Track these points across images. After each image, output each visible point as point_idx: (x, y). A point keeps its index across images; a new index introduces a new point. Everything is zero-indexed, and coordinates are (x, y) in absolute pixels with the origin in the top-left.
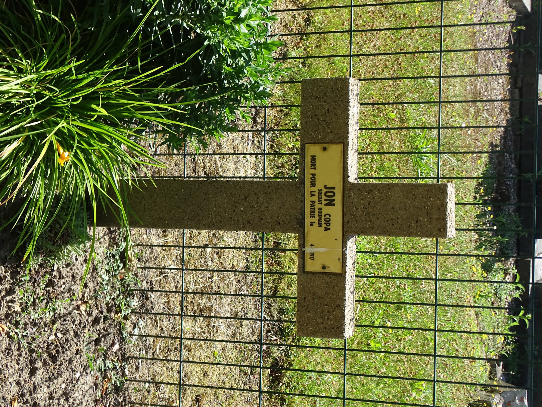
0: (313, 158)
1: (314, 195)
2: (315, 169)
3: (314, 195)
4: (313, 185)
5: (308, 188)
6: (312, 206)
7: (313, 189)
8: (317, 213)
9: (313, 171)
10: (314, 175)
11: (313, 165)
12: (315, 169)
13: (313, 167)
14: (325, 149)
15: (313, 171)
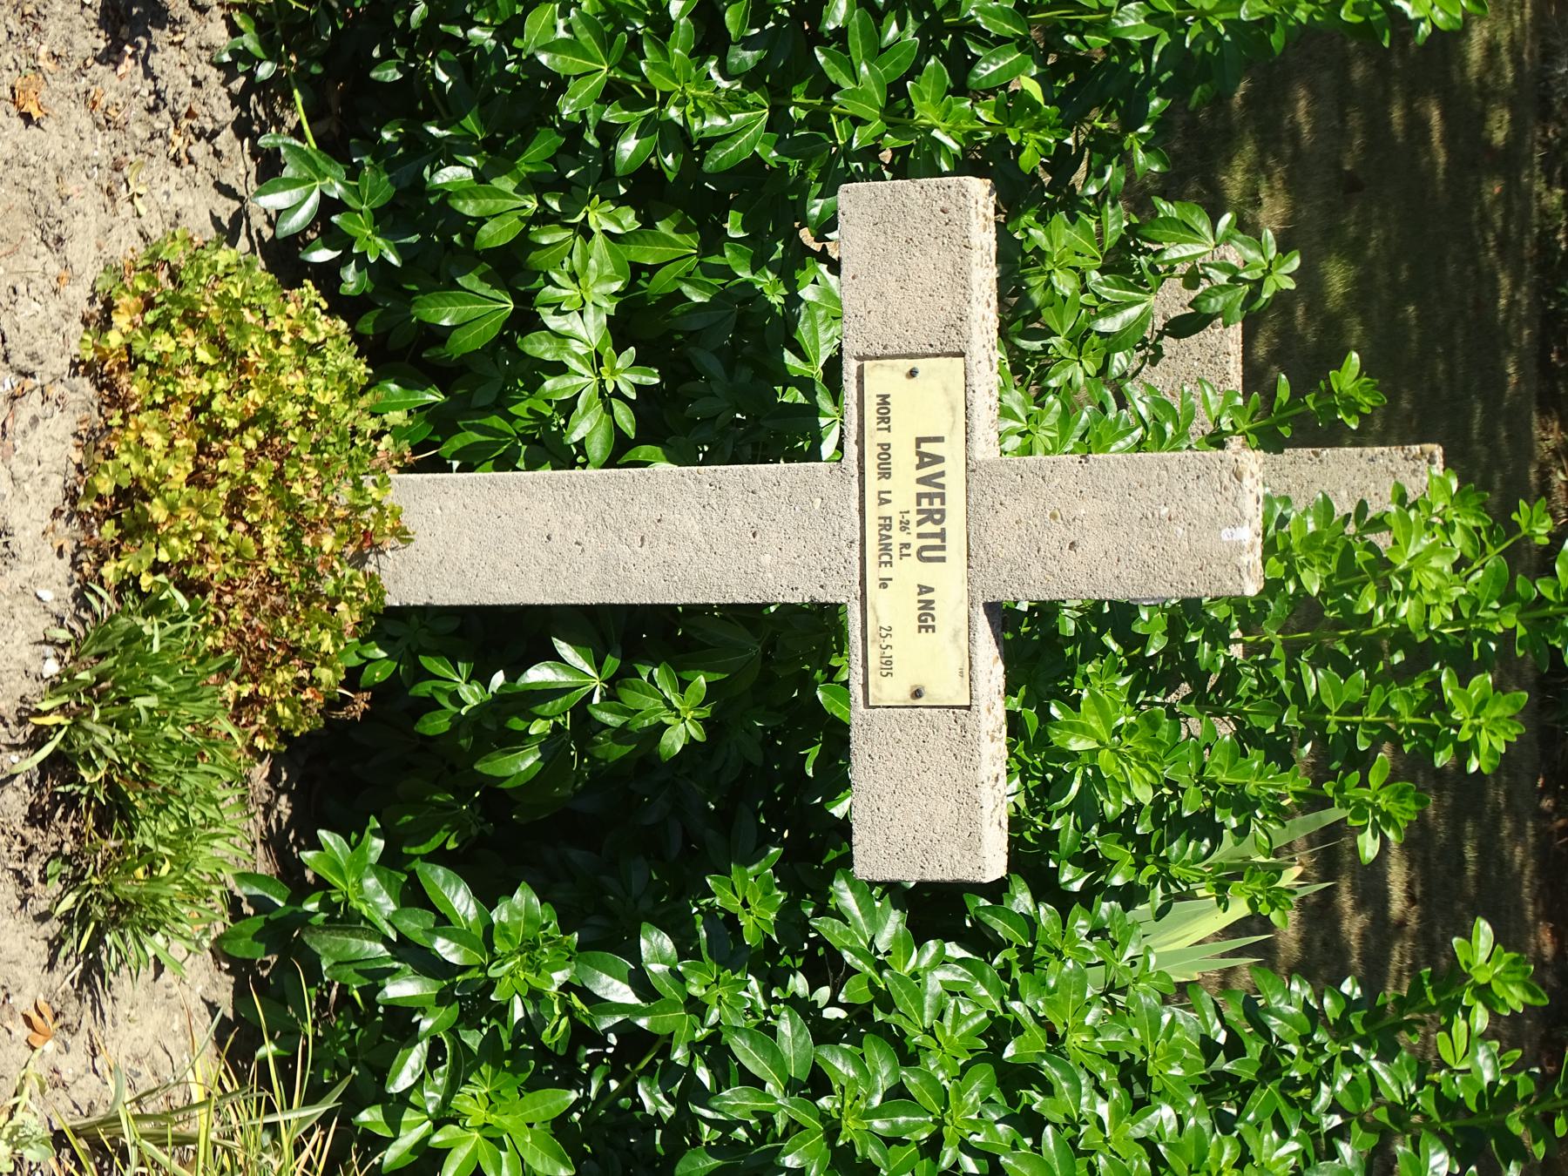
0: (884, 400)
1: (888, 501)
2: (889, 429)
3: (888, 501)
4: (885, 474)
5: (873, 483)
6: (883, 527)
7: (885, 484)
8: (895, 552)
9: (883, 437)
10: (885, 448)
11: (884, 418)
12: (889, 429)
13: (883, 425)
14: (912, 373)
15: (883, 437)
